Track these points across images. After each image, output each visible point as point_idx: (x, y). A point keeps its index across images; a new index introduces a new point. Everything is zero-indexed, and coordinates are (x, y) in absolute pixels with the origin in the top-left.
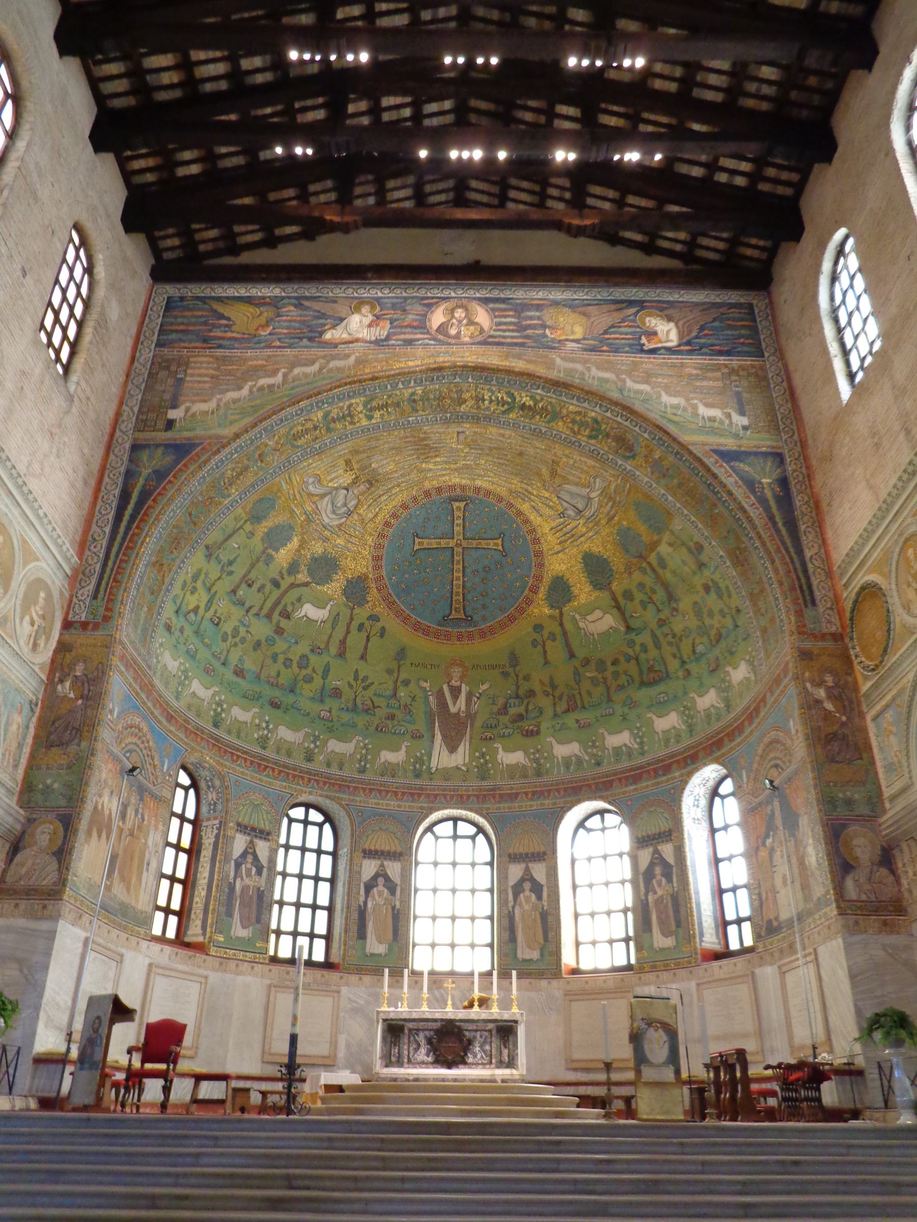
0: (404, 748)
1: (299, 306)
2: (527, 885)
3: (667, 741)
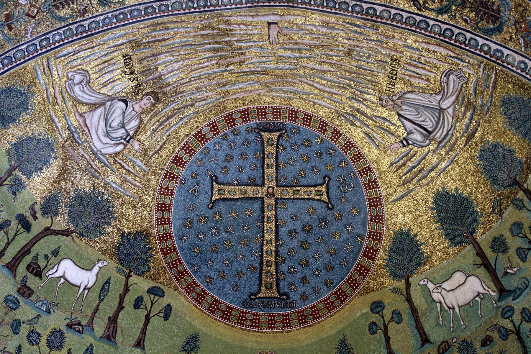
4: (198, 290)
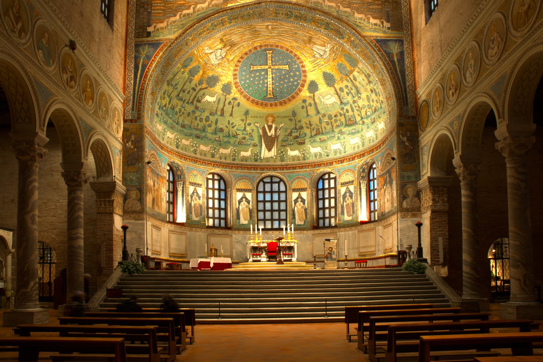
4: (248, 97)
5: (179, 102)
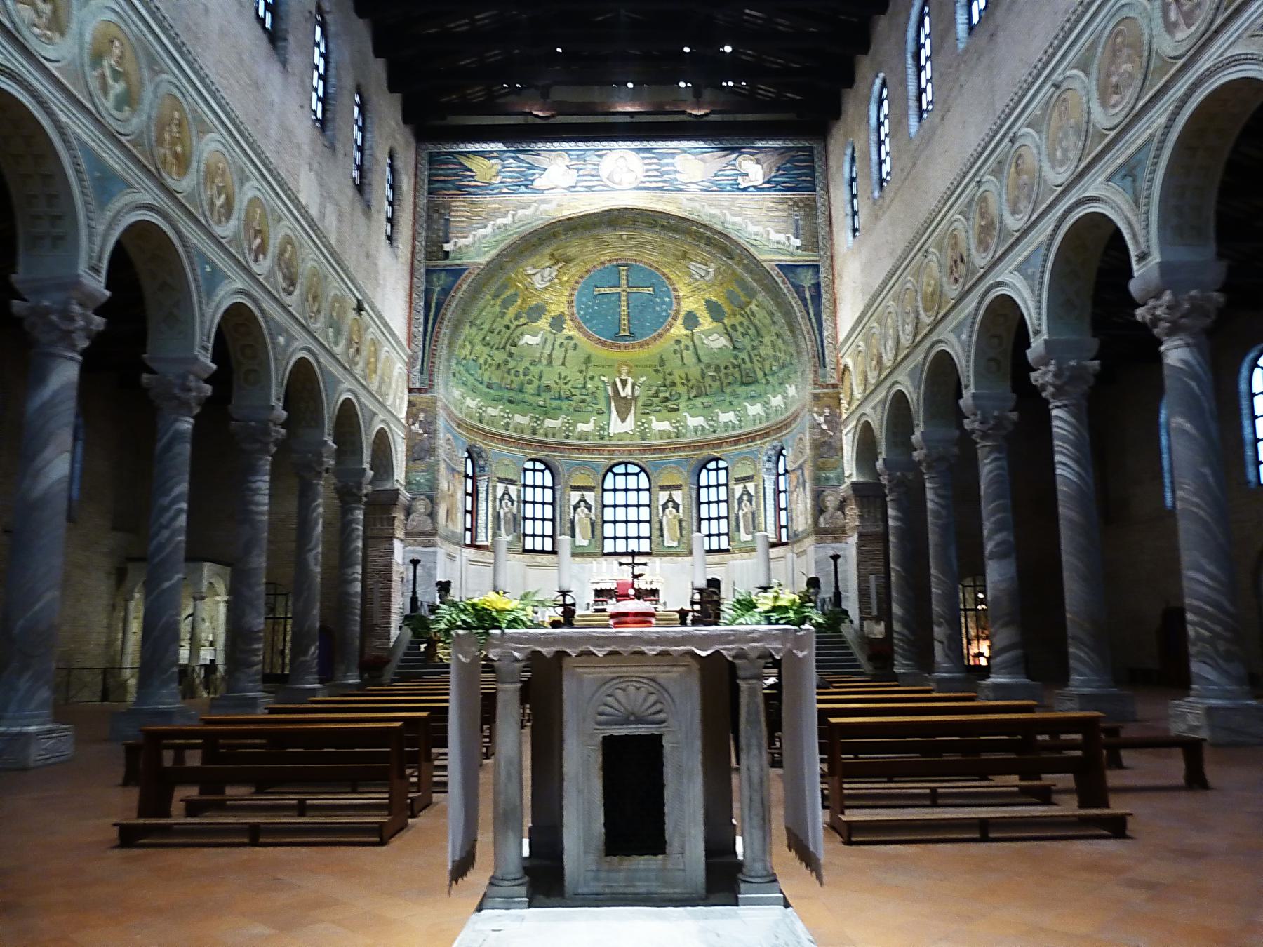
0: (592, 421)
1: (515, 158)
2: (670, 504)
3: (754, 421)
5: (484, 348)
